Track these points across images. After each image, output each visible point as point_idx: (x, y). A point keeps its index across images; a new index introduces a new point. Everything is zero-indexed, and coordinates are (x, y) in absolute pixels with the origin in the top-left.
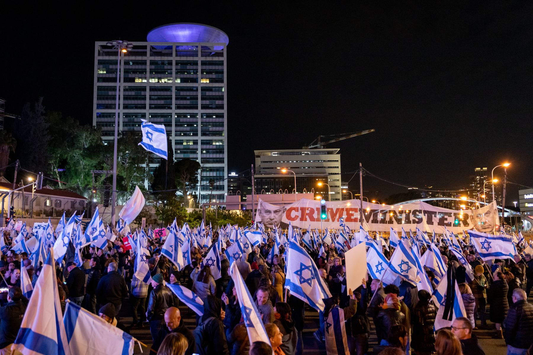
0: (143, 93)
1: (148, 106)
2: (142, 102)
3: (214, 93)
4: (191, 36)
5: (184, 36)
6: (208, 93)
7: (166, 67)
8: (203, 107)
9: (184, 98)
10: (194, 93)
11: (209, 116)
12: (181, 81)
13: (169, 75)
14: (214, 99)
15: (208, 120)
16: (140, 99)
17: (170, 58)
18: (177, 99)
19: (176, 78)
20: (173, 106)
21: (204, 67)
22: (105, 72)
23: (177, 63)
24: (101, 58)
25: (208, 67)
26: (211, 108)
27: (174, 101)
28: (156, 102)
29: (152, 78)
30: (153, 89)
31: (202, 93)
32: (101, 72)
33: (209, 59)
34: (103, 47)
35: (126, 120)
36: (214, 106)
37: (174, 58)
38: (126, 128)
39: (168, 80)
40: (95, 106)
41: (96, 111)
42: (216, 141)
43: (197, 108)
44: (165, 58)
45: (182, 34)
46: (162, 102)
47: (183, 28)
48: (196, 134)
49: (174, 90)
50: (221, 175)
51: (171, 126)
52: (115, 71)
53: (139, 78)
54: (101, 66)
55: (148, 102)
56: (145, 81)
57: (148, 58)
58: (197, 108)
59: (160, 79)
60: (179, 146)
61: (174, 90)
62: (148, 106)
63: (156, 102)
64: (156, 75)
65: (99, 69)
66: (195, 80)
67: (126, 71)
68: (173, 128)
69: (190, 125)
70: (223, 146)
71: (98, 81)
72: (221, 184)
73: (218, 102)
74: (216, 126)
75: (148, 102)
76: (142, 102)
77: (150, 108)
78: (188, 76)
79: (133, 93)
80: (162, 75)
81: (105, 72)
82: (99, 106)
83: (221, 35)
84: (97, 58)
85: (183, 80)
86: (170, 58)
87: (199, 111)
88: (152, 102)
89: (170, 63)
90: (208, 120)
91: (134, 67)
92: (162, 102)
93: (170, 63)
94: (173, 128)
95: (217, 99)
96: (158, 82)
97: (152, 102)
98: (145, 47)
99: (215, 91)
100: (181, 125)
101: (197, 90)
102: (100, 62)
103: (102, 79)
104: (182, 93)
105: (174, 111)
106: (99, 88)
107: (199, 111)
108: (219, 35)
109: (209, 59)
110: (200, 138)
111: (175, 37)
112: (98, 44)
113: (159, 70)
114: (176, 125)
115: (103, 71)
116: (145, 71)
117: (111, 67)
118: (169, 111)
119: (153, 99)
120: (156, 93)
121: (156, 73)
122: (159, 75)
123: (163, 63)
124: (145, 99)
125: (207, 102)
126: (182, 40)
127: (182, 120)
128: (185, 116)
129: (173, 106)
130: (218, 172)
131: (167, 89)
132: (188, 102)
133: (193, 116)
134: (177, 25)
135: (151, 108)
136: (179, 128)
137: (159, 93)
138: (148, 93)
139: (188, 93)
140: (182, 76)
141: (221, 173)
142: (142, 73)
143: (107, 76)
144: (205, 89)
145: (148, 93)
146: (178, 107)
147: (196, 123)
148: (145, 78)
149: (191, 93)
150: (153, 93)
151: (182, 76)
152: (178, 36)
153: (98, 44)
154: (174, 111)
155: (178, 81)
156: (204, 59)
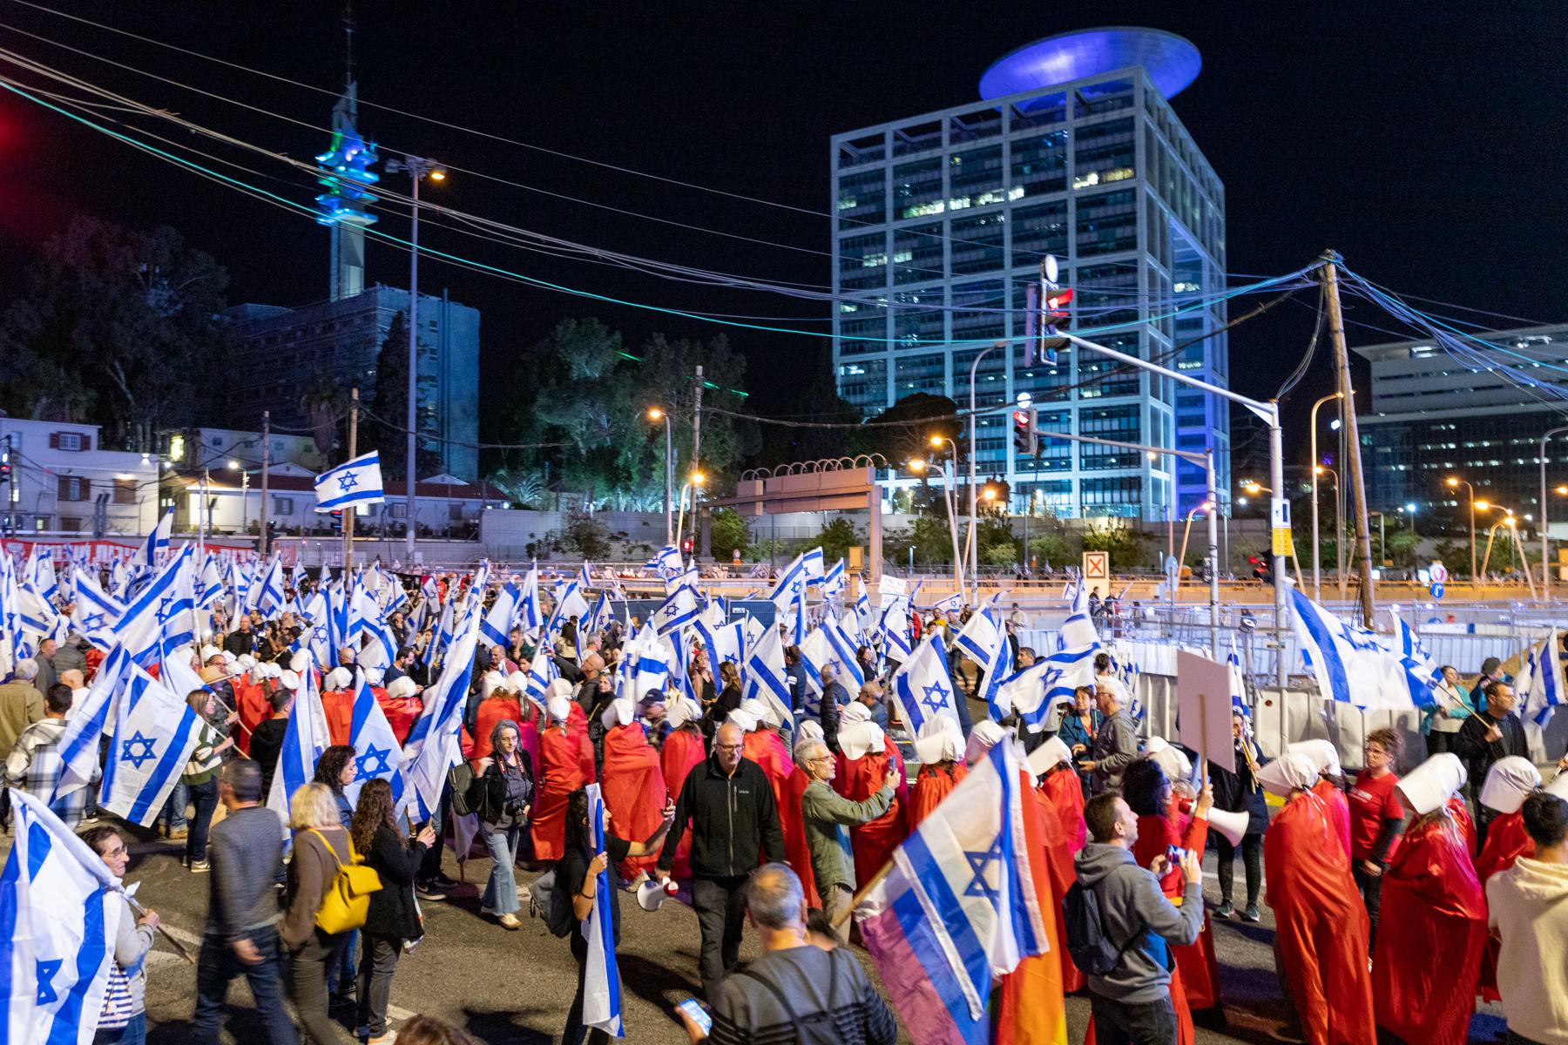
3: (1110, 211)
4: (1078, 67)
5: (1058, 73)
6: (1094, 213)
7: (988, 164)
12: (1027, 194)
14: (1110, 225)
16: (930, 255)
18: (1017, 240)
19: (1013, 187)
20: (1008, 260)
21: (1084, 145)
22: (853, 205)
23: (1016, 148)
24: (845, 172)
25: (1092, 143)
26: (1105, 251)
27: (1008, 248)
29: (956, 198)
30: (961, 223)
31: (1078, 216)
34: (858, 143)
36: (1112, 245)
37: (1006, 138)
45: (1057, 64)
46: (981, 254)
50: (1133, 426)
52: (879, 197)
54: (846, 191)
55: (947, 258)
59: (974, 197)
65: (841, 199)
66: (1061, 184)
71: (841, 228)
72: (1064, 454)
75: (947, 258)
80: (980, 186)
83: (1163, 44)
84: (837, 172)
85: (1030, 191)
89: (996, 152)
93: (996, 152)
95: (1119, 224)
96: (972, 205)
99: (1116, 203)
101: (1065, 210)
102: (846, 183)
103: (849, 221)
104: (1027, 224)
106: (846, 244)
108: (1156, 45)
109: (1095, 119)
111: (1035, 78)
112: (838, 141)
113: (975, 176)
117: (866, 188)
122: (973, 189)
124: (940, 253)
129: (1008, 260)
130: (1124, 420)
131: (991, 215)
134: (1031, 48)
138: (947, 239)
141: (1133, 419)
142: (930, 191)
144: (1088, 202)
145: (947, 239)
148: (940, 198)
151: (1028, 180)
152: (1043, 74)
153: (838, 141)
155: (1019, 192)
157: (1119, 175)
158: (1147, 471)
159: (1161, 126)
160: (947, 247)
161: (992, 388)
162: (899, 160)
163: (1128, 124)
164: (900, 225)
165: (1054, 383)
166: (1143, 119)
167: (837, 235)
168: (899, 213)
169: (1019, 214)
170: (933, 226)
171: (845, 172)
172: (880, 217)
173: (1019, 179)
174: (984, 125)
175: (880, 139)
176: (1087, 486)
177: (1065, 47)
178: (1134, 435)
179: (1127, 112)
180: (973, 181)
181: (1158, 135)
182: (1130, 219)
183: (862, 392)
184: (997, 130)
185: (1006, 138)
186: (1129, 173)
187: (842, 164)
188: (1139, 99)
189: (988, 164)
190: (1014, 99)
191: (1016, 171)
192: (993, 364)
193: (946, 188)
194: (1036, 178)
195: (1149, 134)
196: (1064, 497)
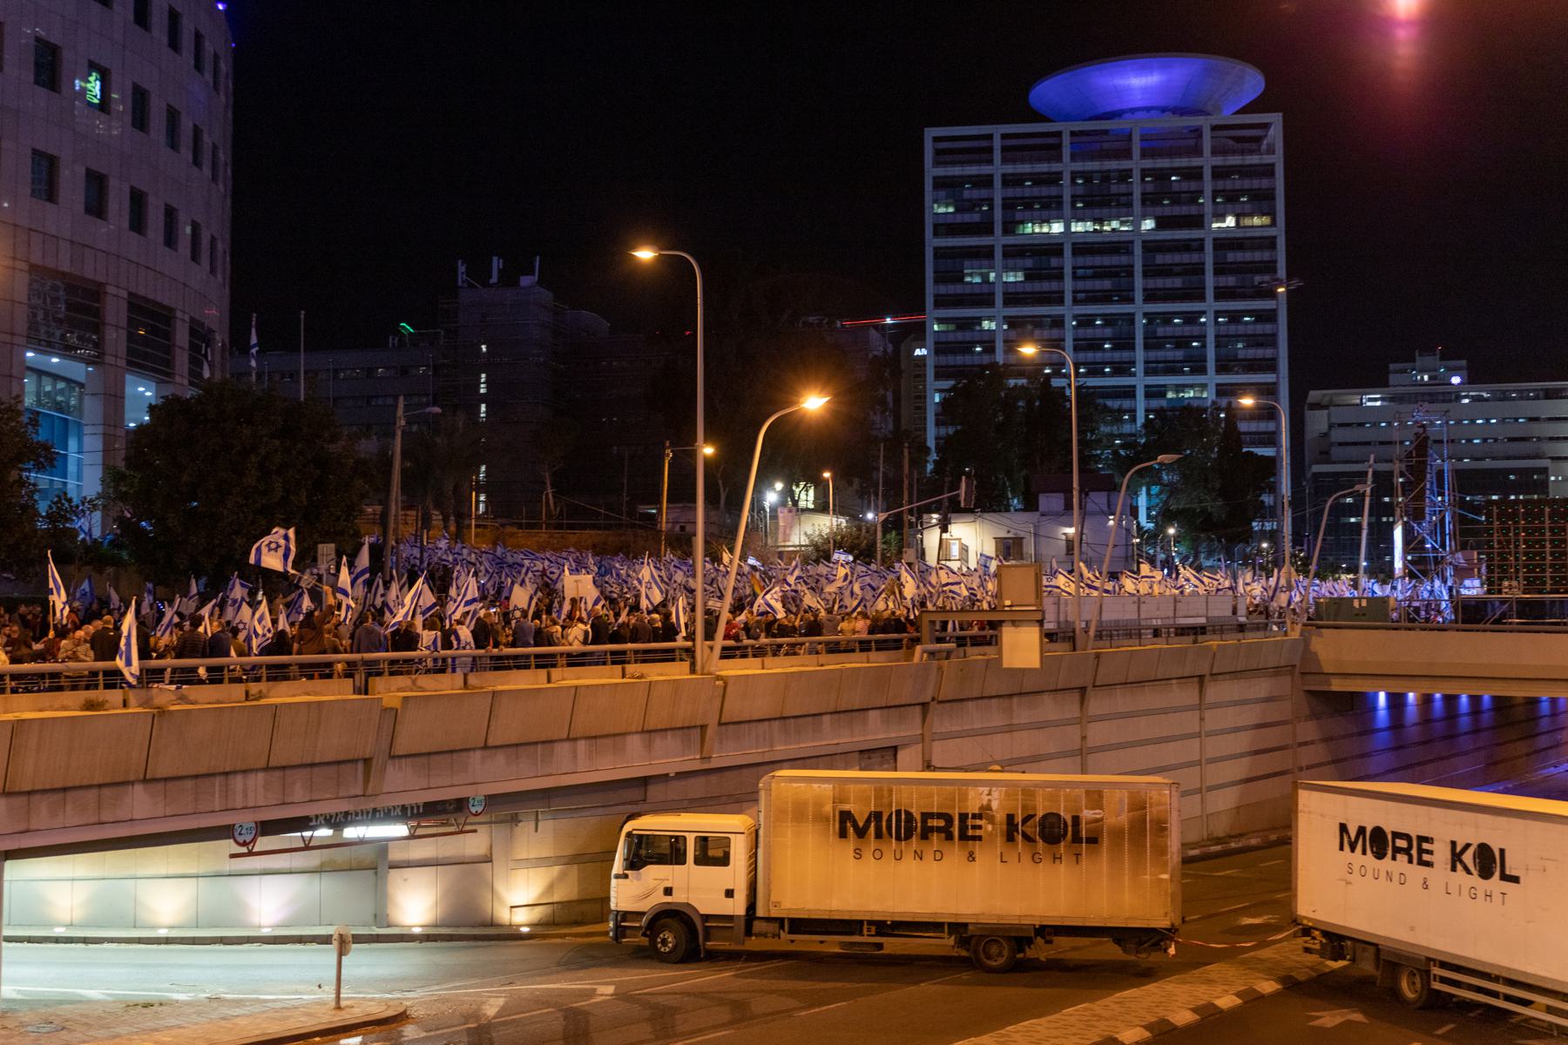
0: (1054, 262)
1: (1068, 297)
2: (1054, 286)
3: (1248, 256)
5: (1145, 90)
6: (1231, 256)
7: (1114, 189)
9: (1165, 271)
10: (1195, 258)
11: (1235, 317)
13: (1124, 210)
15: (1232, 329)
16: (1049, 278)
17: (1125, 164)
19: (1144, 217)
20: (1139, 295)
22: (951, 210)
23: (1145, 173)
24: (941, 171)
26: (1244, 297)
28: (1089, 285)
29: (1079, 220)
31: (1215, 257)
32: (942, 210)
39: (1122, 223)
43: (1202, 298)
44: (1113, 165)
45: (1139, 82)
46: (1107, 284)
48: (1200, 369)
49: (1138, 250)
54: (942, 193)
55: (1068, 285)
58: (1202, 298)
61: (1138, 250)
62: (1068, 297)
63: (1089, 285)
64: (1088, 212)
65: (935, 201)
66: (1197, 222)
67: (1009, 205)
69: (1182, 342)
71: (936, 234)
74: (1260, 345)
75: (1068, 285)
76: (1054, 286)
77: (1076, 301)
78: (1177, 210)
80: (1106, 211)
84: (931, 171)
86: (1125, 164)
87: (1210, 304)
88: (1081, 285)
90: (1232, 329)
91: (1036, 191)
92: (1107, 284)
97: (1081, 285)
100: (1160, 347)
101: (1201, 248)
102: (940, 183)
103: (945, 228)
104: (1160, 259)
105: (1139, 308)
107: (1210, 304)
111: (1120, 92)
112: (930, 133)
113: (1098, 201)
114: (1147, 347)
115: (947, 206)
118: (1126, 308)
119: (1083, 278)
120: (1089, 260)
121: (1088, 205)
122: (1097, 212)
123: (1106, 177)
124: (1060, 277)
127: (1161, 331)
128: (1167, 318)
129: (1139, 295)
131: (1118, 246)
132: (1178, 282)
133: (1191, 318)
135: (1076, 301)
136: (1153, 355)
137: (1098, 260)
138: (1068, 262)
139: (1177, 258)
140: (1158, 210)
142: (1051, 208)
143: (960, 218)
145: (1068, 262)
146: (1150, 296)
147: (1202, 338)
148: (1058, 218)
149: (1186, 258)
150: (1080, 261)
152: (1129, 89)
154: (1139, 308)
155: (1148, 224)
157: (1256, 221)
160: (1068, 271)
164: (1010, 240)
167: (932, 242)
168: (1010, 227)
169: (1151, 247)
170: (1052, 248)
172: (986, 228)
180: (1104, 204)
186: (1266, 220)
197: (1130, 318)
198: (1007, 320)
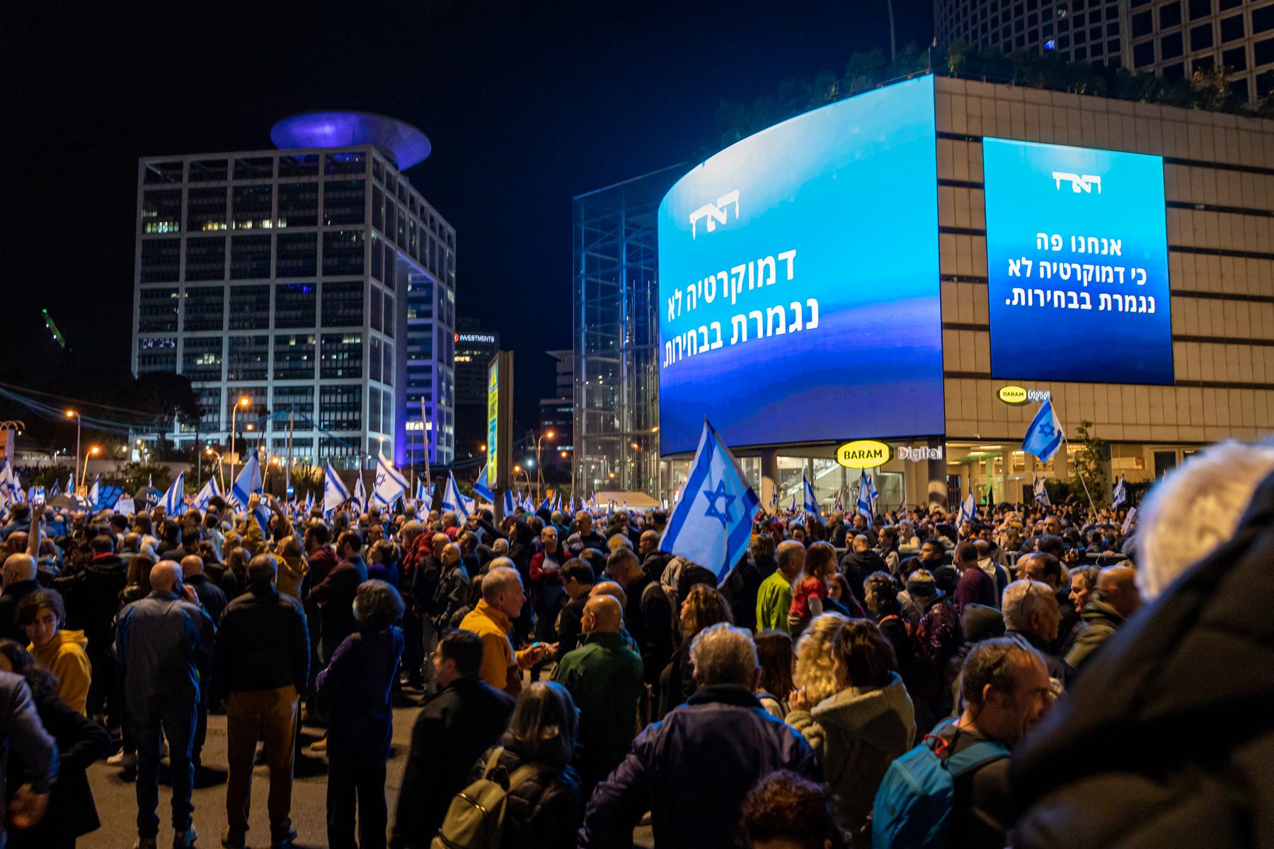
7: (262, 198)
8: (326, 272)
24: (149, 187)
30: (237, 240)
33: (338, 178)
35: (191, 301)
37: (275, 181)
38: (190, 317)
40: (138, 277)
41: (139, 286)
42: (349, 336)
43: (314, 274)
45: (326, 131)
47: (319, 122)
51: (267, 308)
53: (214, 222)
55: (228, 265)
56: (224, 227)
57: (230, 183)
58: (314, 274)
60: (282, 348)
67: (193, 210)
68: (272, 313)
70: (361, 344)
73: (353, 261)
79: (203, 250)
81: (155, 214)
82: (147, 277)
84: (142, 188)
94: (272, 313)
98: (269, 161)
102: (149, 196)
107: (319, 280)
109: (338, 178)
110: (319, 330)
112: (147, 163)
113: (253, 206)
114: (278, 308)
116: (222, 209)
125: (335, 261)
126: (324, 144)
130: (351, 396)
131: (265, 238)
151: (290, 214)
156: (329, 178)
158: (365, 433)
159: (390, 187)
161: (258, 366)
162: (194, 185)
163: (361, 185)
165: (304, 366)
166: (372, 181)
169: (283, 239)
170: (218, 240)
171: (149, 187)
173: (284, 213)
174: (260, 168)
175: (179, 166)
176: (324, 443)
177: (331, 121)
178: (357, 407)
179: (361, 177)
181: (387, 194)
182: (360, 252)
183: (155, 363)
184: (269, 175)
185: (275, 181)
187: (146, 182)
188: (370, 168)
189: (262, 198)
190: (283, 153)
191: (282, 207)
192: (259, 348)
193: (229, 213)
194: (296, 213)
195: (376, 193)
196: (308, 450)
197: (266, 289)
198: (187, 290)
